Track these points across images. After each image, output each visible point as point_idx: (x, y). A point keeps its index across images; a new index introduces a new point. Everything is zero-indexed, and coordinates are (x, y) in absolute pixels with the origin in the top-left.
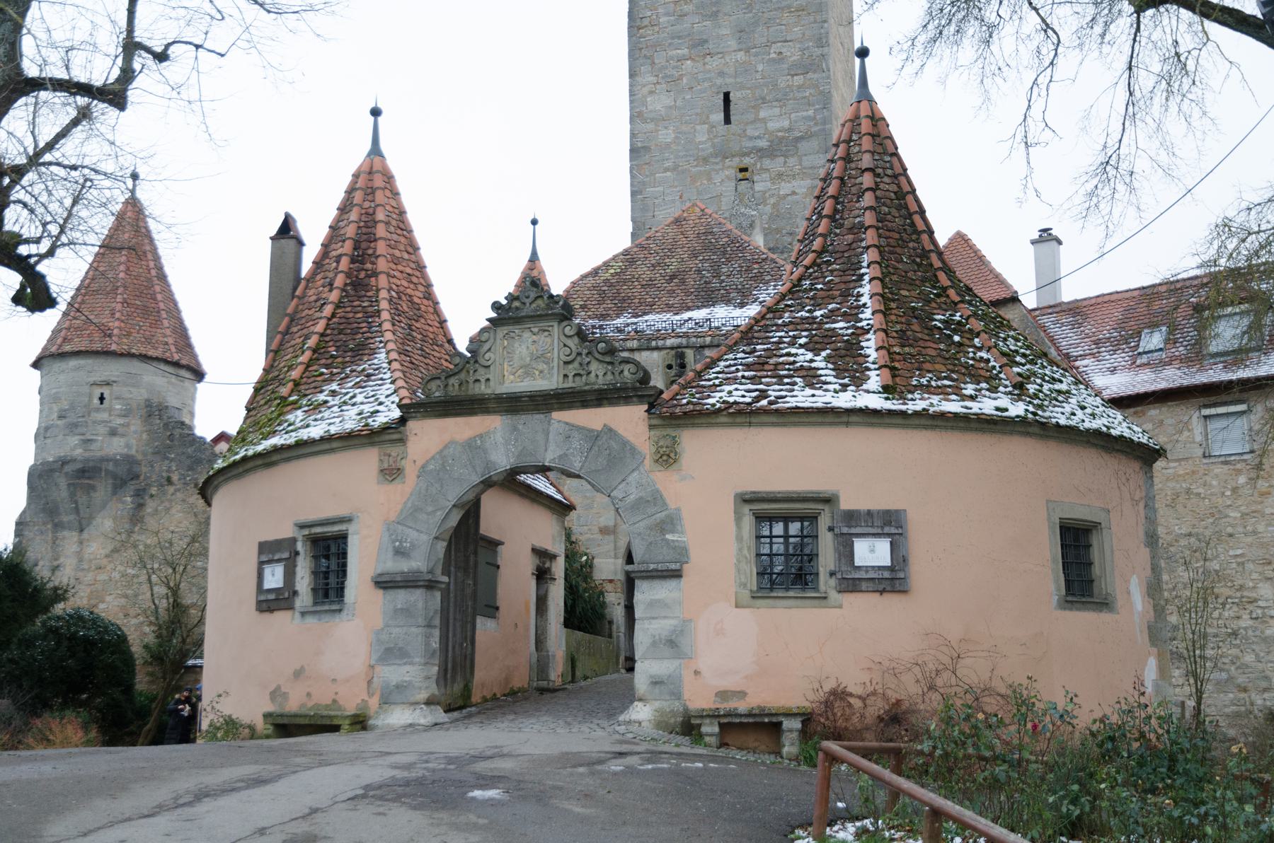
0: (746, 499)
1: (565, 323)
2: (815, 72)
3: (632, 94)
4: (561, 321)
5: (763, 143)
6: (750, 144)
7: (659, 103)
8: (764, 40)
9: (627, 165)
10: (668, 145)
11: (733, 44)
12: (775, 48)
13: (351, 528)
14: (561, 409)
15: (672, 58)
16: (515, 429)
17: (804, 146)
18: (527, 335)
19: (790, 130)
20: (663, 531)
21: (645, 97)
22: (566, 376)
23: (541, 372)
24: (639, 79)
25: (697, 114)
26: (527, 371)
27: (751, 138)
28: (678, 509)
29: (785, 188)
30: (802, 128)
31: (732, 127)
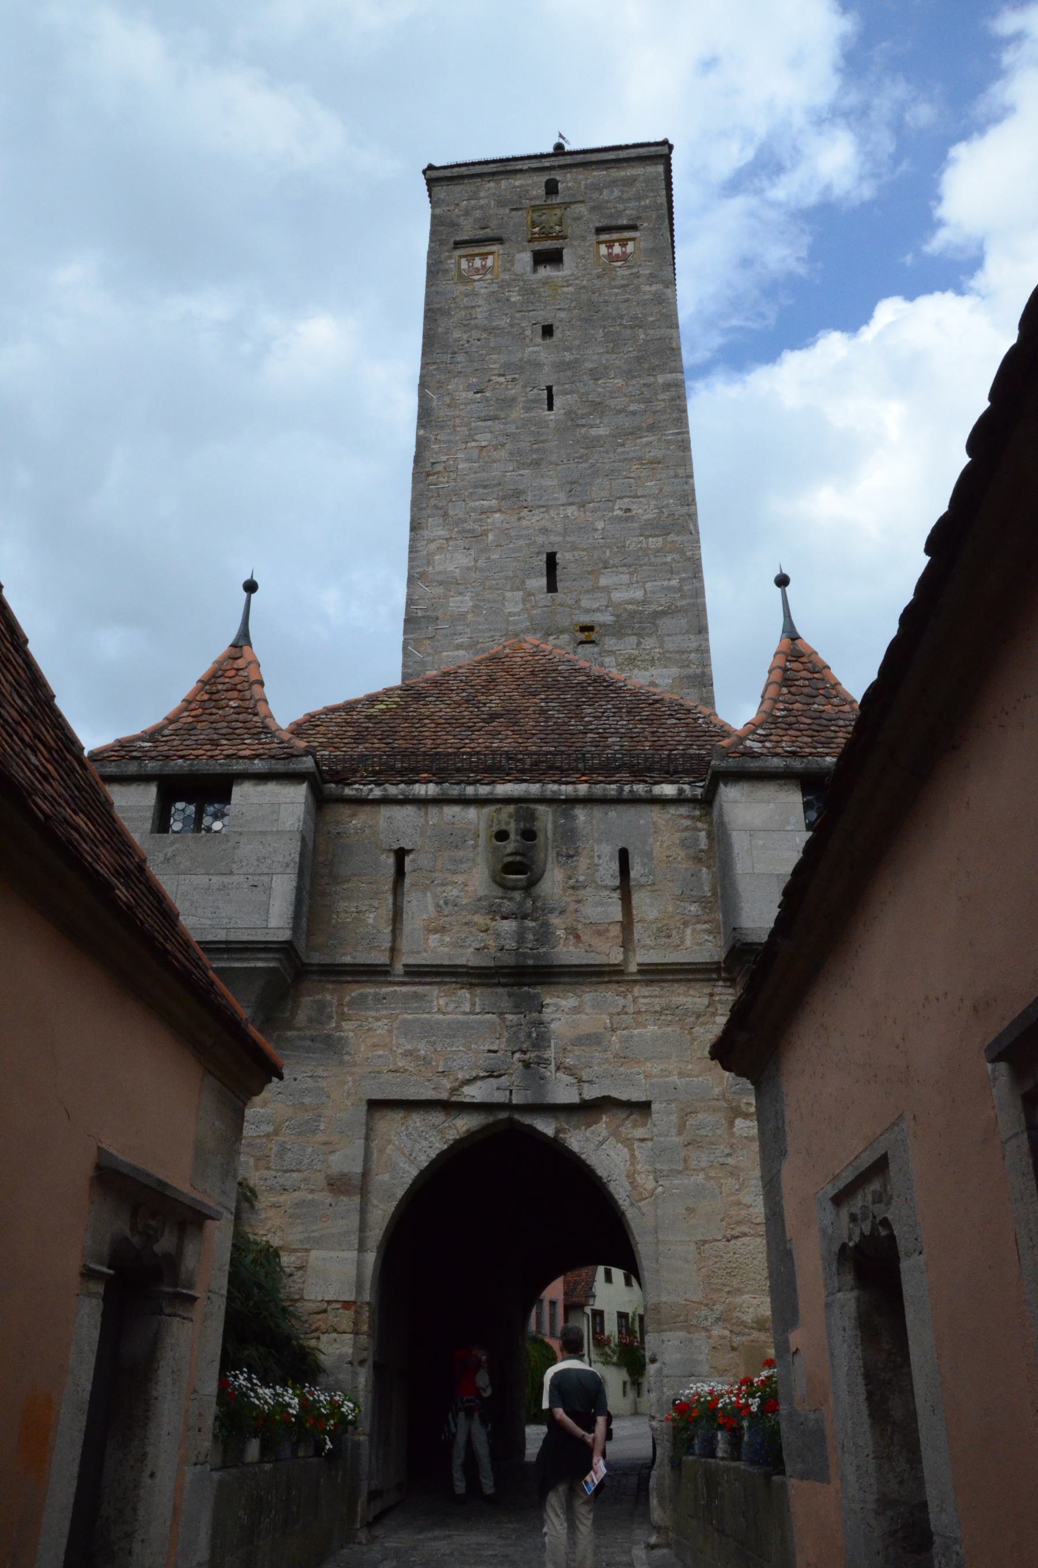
2: (678, 533)
3: (412, 549)
7: (454, 562)
8: (605, 494)
9: (400, 638)
10: (463, 616)
11: (563, 498)
12: (619, 504)
15: (474, 510)
17: (666, 624)
19: (644, 602)
21: (433, 554)
24: (426, 533)
25: (507, 578)
27: (588, 611)
31: (559, 596)
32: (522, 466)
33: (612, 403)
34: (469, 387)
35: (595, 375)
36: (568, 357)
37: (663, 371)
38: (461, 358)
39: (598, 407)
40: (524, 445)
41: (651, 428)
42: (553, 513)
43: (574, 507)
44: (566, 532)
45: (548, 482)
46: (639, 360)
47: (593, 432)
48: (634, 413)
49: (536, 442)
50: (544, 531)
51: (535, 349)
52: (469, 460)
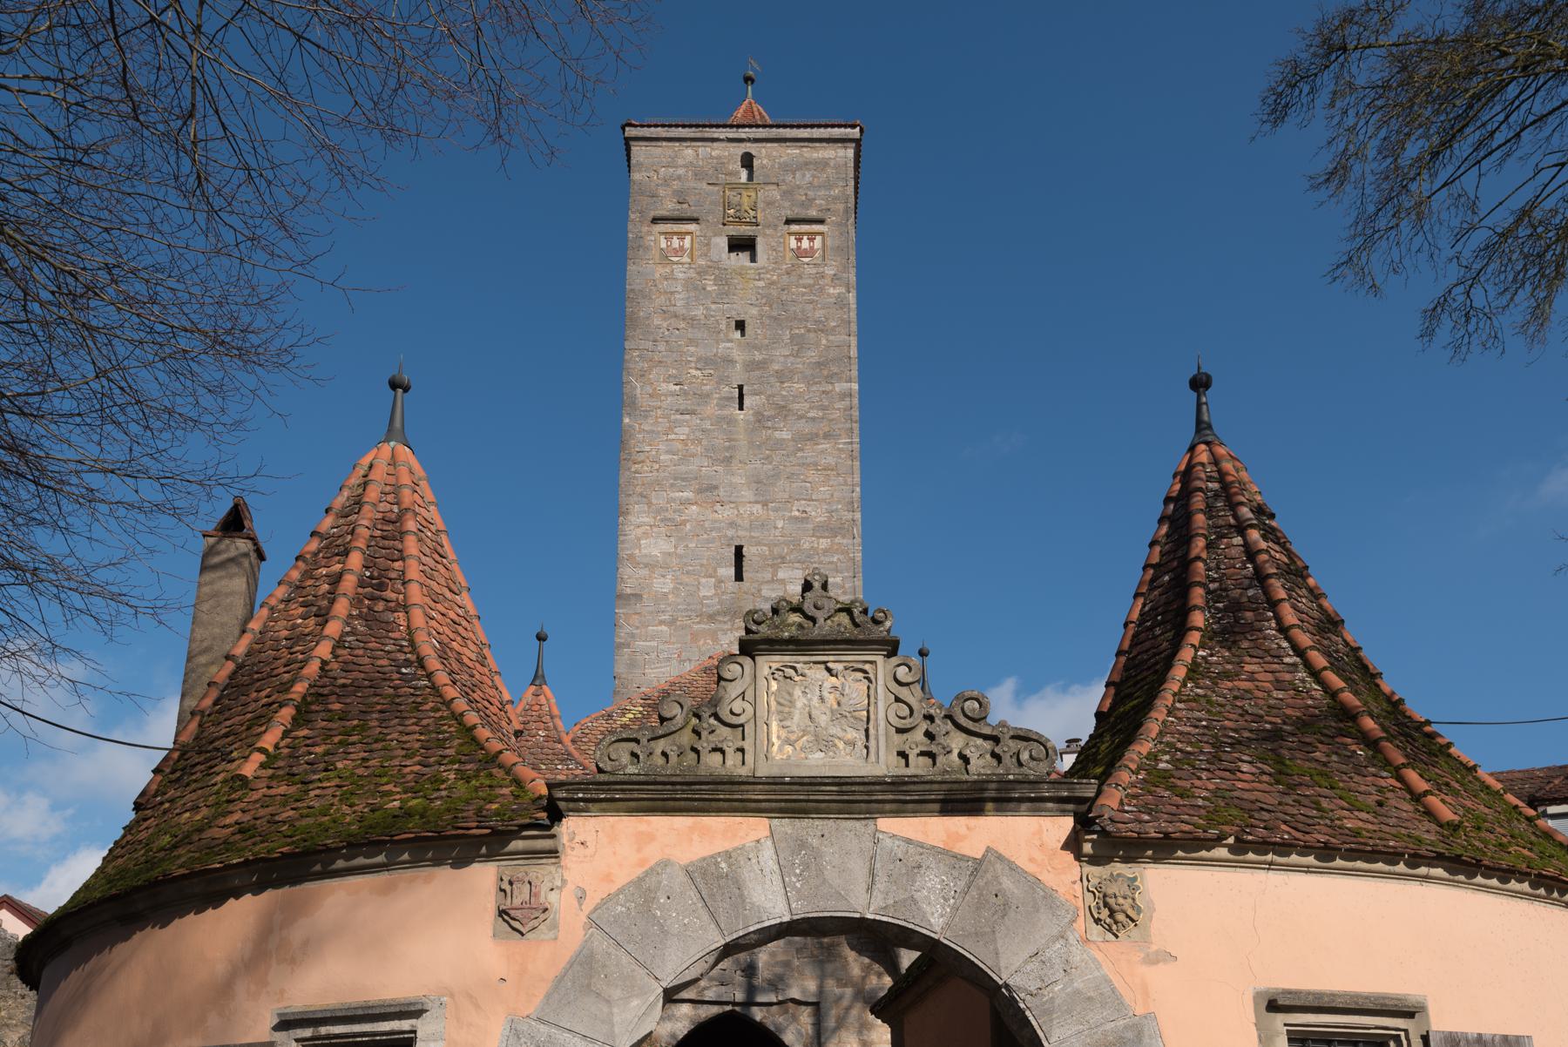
1: (894, 660)
4: (888, 656)
11: (748, 494)
13: (423, 1027)
14: (897, 813)
16: (802, 845)
18: (819, 673)
22: (903, 755)
23: (852, 744)
26: (824, 743)
28: (1150, 1016)
32: (715, 461)
33: (796, 406)
34: (667, 380)
35: (781, 377)
36: (758, 357)
37: (839, 380)
38: (662, 347)
39: (783, 411)
41: (827, 436)
43: (759, 506)
44: (751, 528)
45: (737, 480)
46: (819, 364)
47: (777, 434)
48: (813, 419)
49: (730, 440)
50: (732, 524)
52: (668, 452)
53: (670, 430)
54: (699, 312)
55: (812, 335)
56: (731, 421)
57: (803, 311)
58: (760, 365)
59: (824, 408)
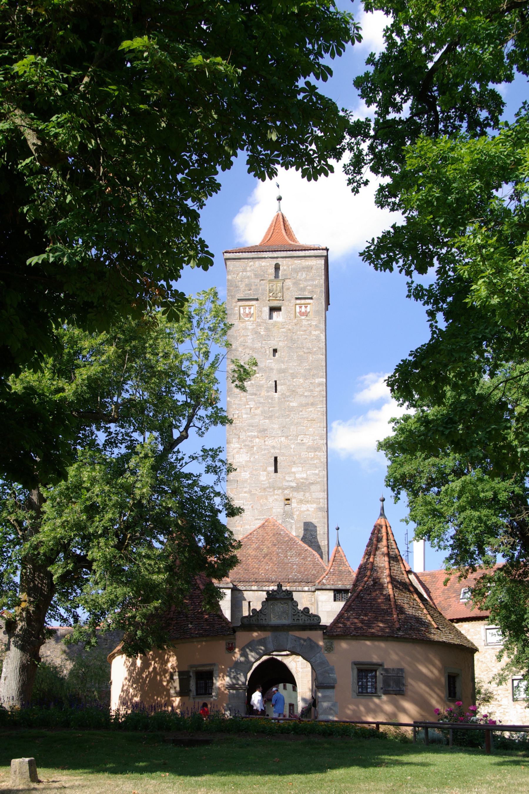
0: (355, 663)
2: (319, 452)
5: (294, 484)
6: (287, 484)
13: (215, 668)
15: (249, 436)
17: (313, 488)
18: (279, 604)
19: (306, 479)
20: (329, 674)
24: (232, 445)
27: (288, 481)
29: (304, 507)
30: (313, 479)
32: (265, 418)
36: (283, 366)
39: (293, 392)
40: (266, 409)
41: (312, 404)
42: (276, 440)
46: (309, 370)
48: (306, 396)
50: (274, 447)
51: (270, 361)
52: (247, 414)
53: (247, 403)
54: (258, 345)
55: (306, 355)
56: (272, 398)
57: (302, 343)
58: (283, 371)
59: (311, 391)
